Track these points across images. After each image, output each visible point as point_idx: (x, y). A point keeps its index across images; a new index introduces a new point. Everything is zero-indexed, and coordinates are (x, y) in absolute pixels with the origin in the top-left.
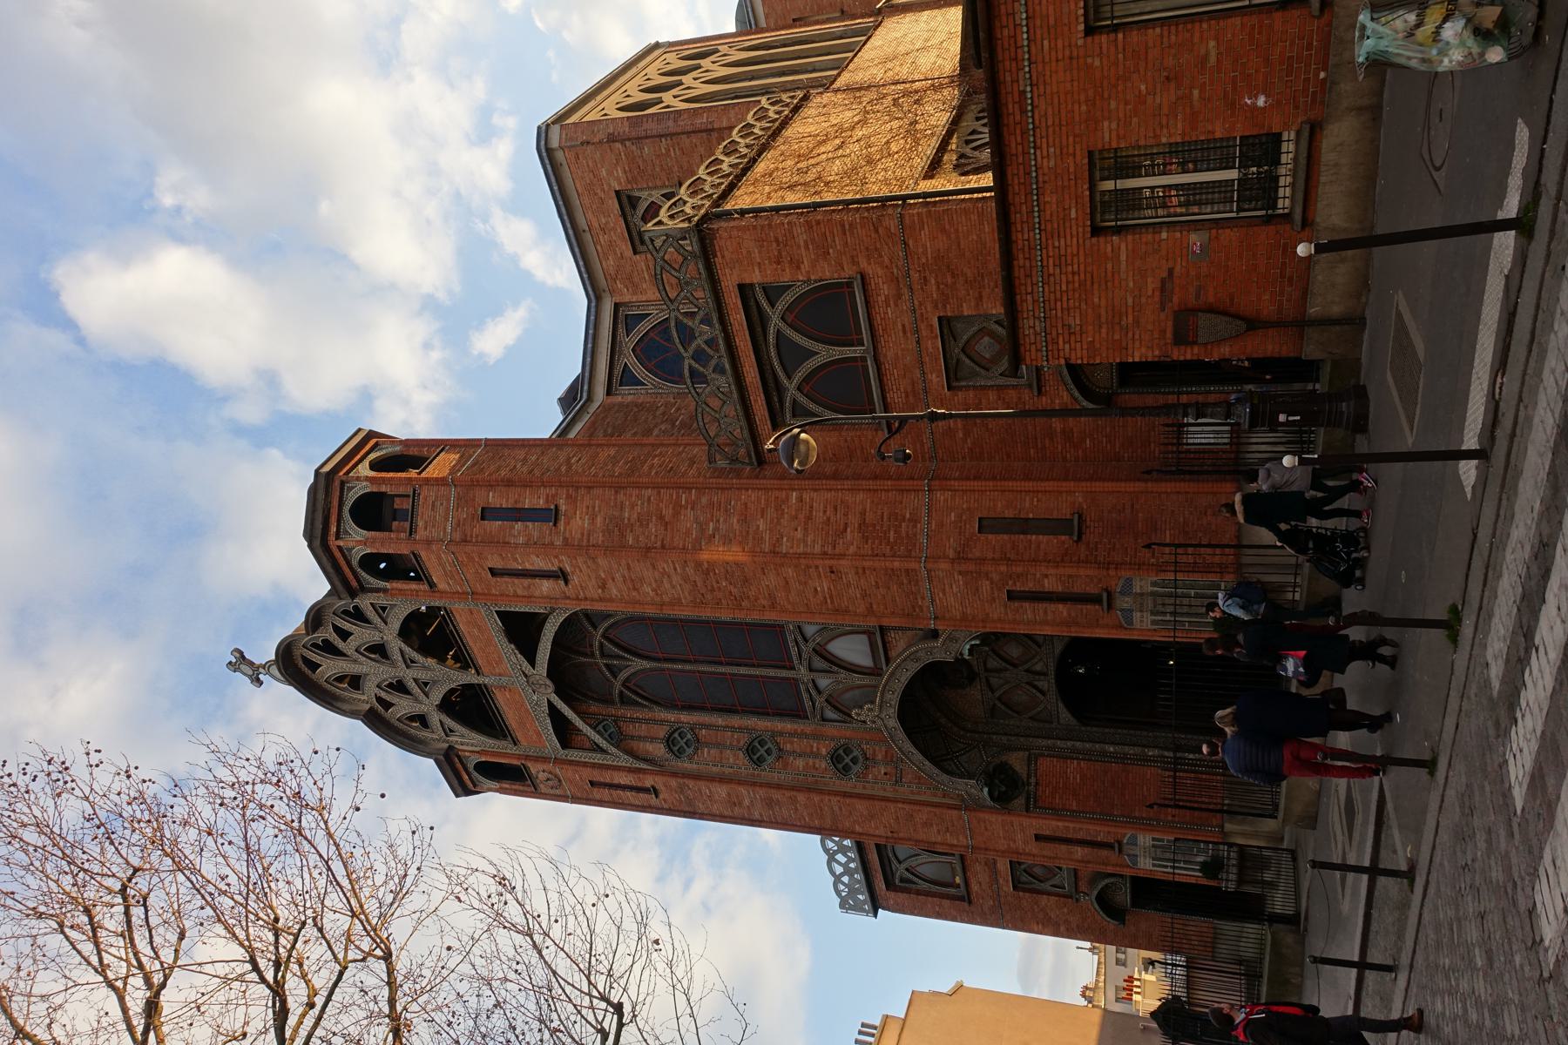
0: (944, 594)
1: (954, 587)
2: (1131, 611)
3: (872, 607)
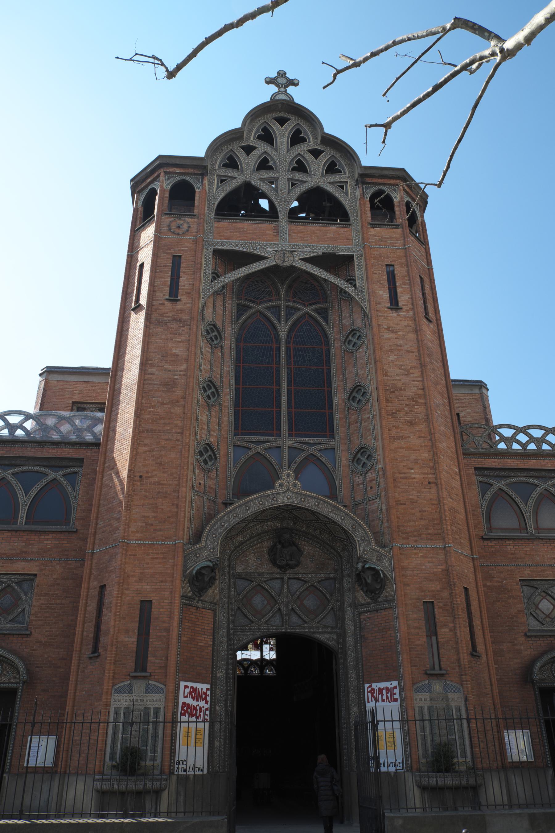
0: (422, 556)
1: (431, 564)
2: (430, 691)
3: (402, 504)
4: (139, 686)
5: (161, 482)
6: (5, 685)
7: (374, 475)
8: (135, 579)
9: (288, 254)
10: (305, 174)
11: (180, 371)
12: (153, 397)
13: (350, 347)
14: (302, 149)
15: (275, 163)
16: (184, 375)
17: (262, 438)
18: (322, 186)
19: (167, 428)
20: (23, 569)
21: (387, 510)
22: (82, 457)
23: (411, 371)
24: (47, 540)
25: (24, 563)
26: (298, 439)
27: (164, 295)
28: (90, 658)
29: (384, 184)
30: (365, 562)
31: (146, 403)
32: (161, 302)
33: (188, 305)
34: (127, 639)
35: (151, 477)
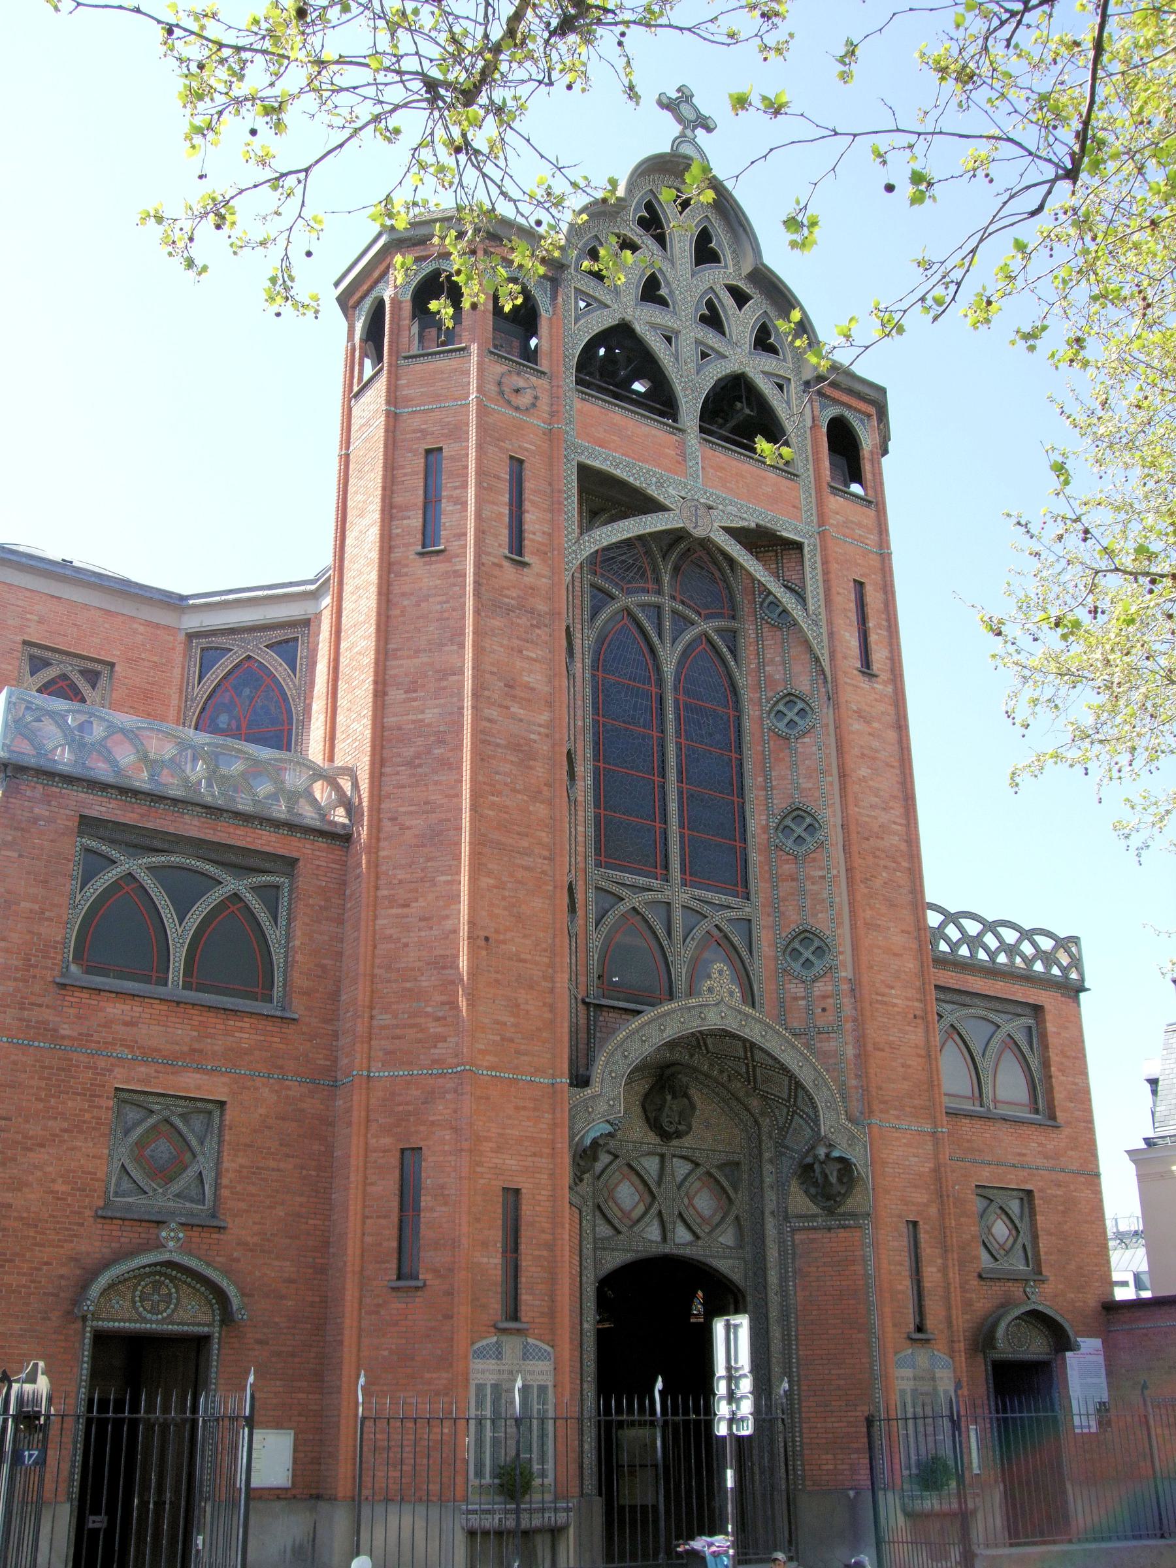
1: (916, 1159)
4: (511, 1345)
5: (523, 956)
6: (116, 1324)
7: (830, 988)
8: (491, 1145)
9: (702, 511)
10: (719, 336)
11: (540, 726)
12: (497, 773)
13: (781, 725)
14: (716, 277)
15: (671, 293)
16: (547, 736)
17: (642, 881)
18: (751, 375)
19: (525, 843)
20: (199, 1088)
21: (857, 1056)
22: (295, 855)
23: (891, 804)
24: (241, 1030)
25: (198, 1076)
26: (697, 892)
27: (500, 545)
28: (393, 1289)
29: (849, 407)
30: (831, 1146)
31: (484, 783)
32: (496, 561)
33: (544, 580)
34: (485, 1260)
35: (504, 942)
